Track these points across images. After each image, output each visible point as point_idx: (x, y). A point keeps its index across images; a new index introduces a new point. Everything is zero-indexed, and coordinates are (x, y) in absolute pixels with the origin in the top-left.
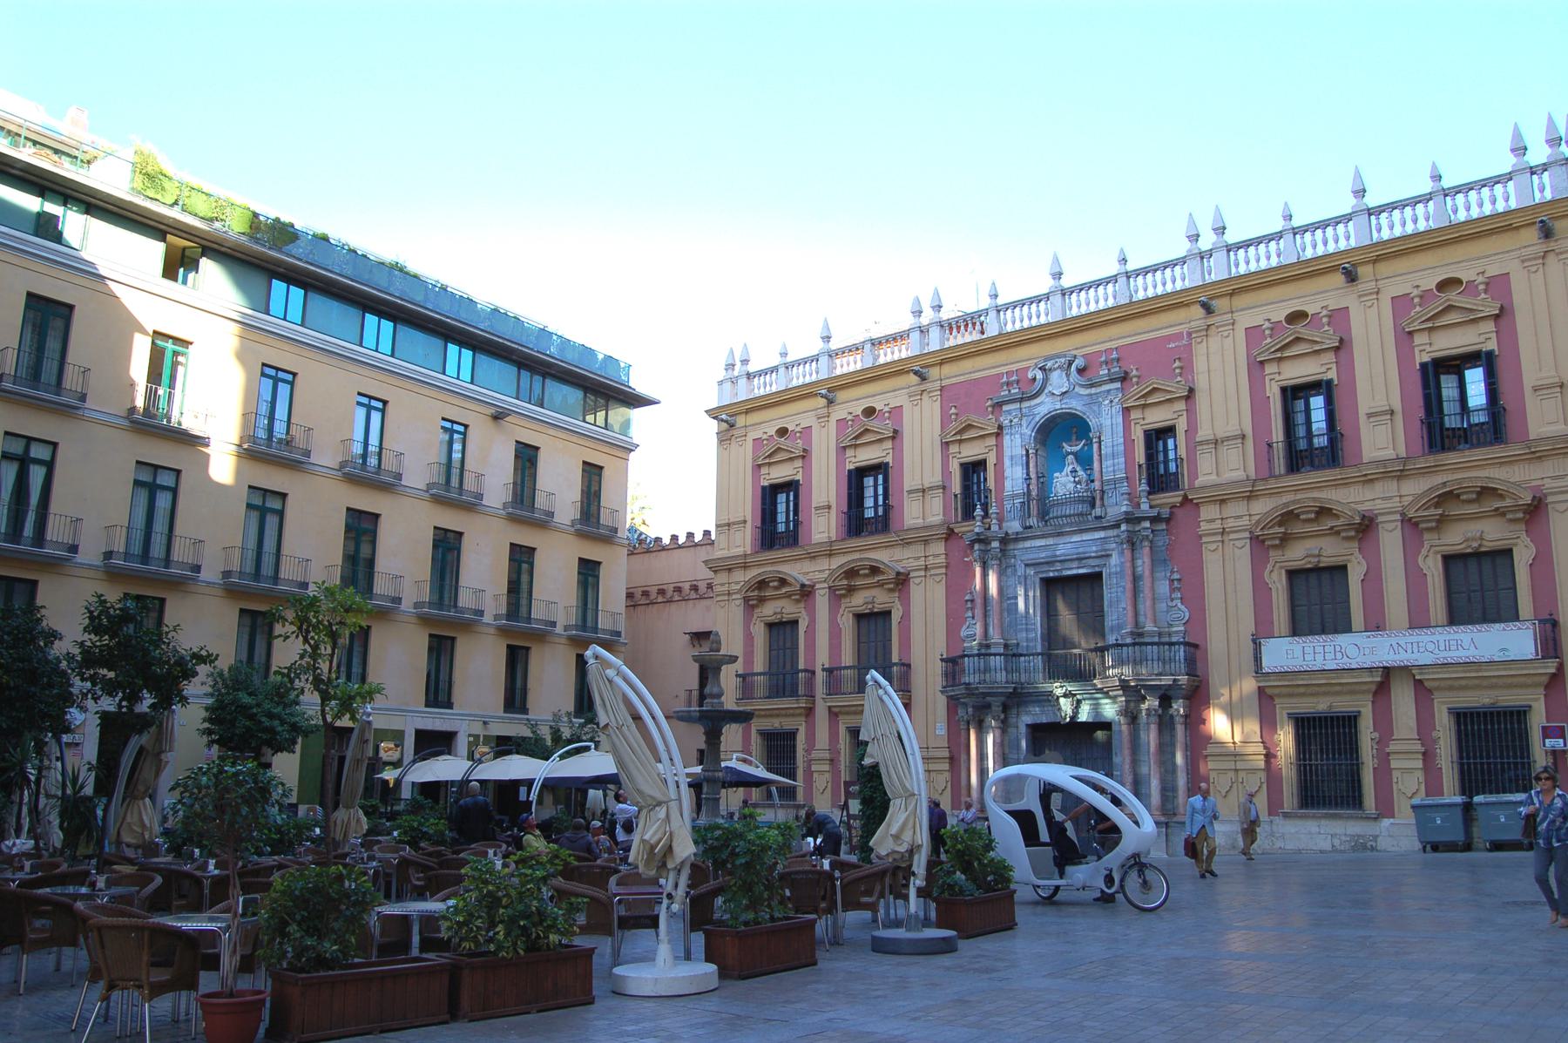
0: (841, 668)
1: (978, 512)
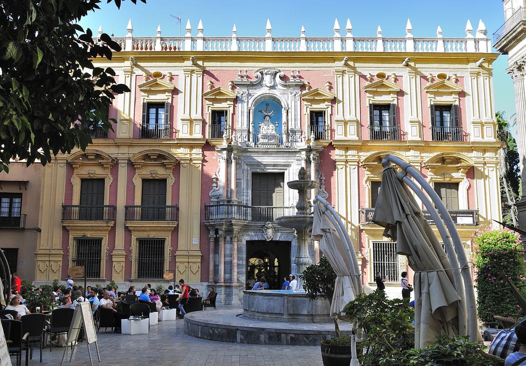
0: (135, 207)
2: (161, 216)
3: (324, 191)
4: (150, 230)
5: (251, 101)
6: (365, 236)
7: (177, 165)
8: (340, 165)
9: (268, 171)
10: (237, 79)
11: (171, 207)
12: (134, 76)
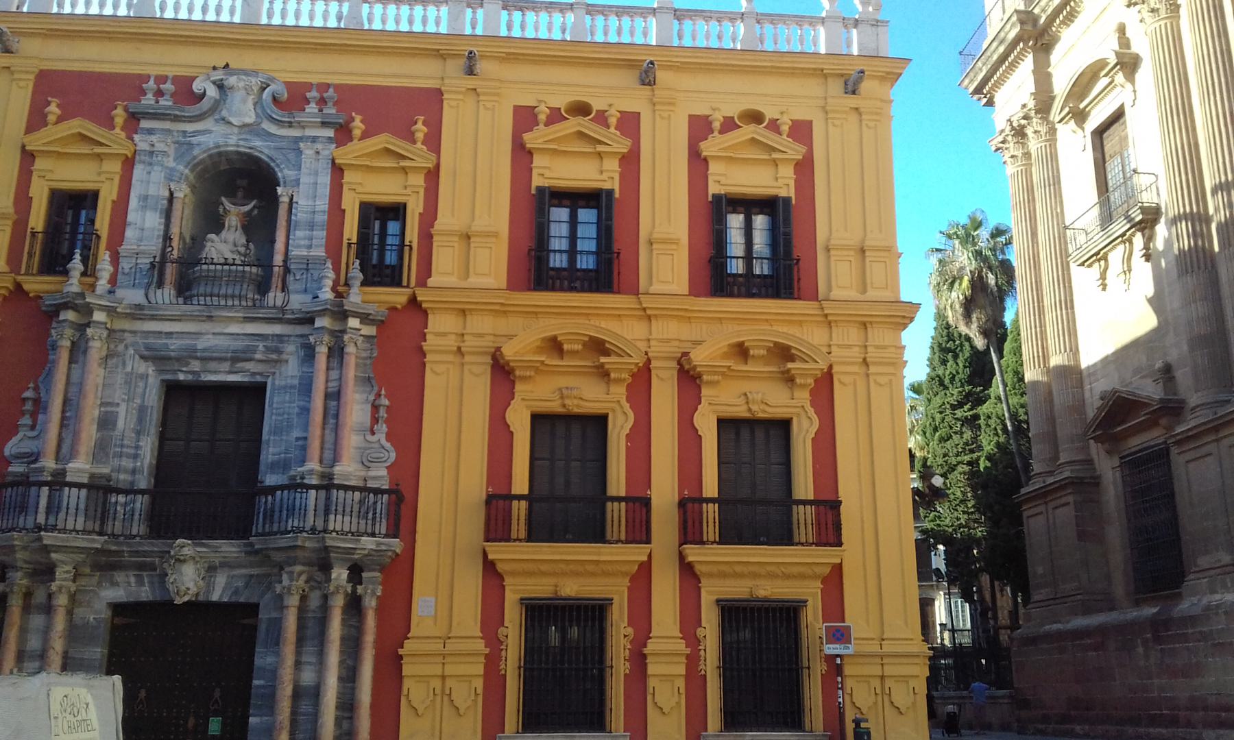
1: (76, 265)
3: (384, 441)
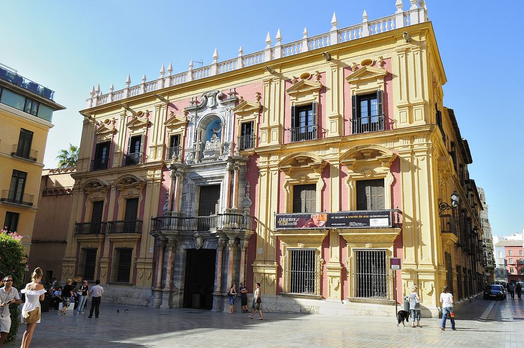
2: (132, 231)
4: (123, 241)
5: (198, 123)
6: (282, 243)
7: (144, 185)
8: (263, 172)
9: (210, 183)
10: (189, 105)
11: (139, 221)
12: (126, 117)
